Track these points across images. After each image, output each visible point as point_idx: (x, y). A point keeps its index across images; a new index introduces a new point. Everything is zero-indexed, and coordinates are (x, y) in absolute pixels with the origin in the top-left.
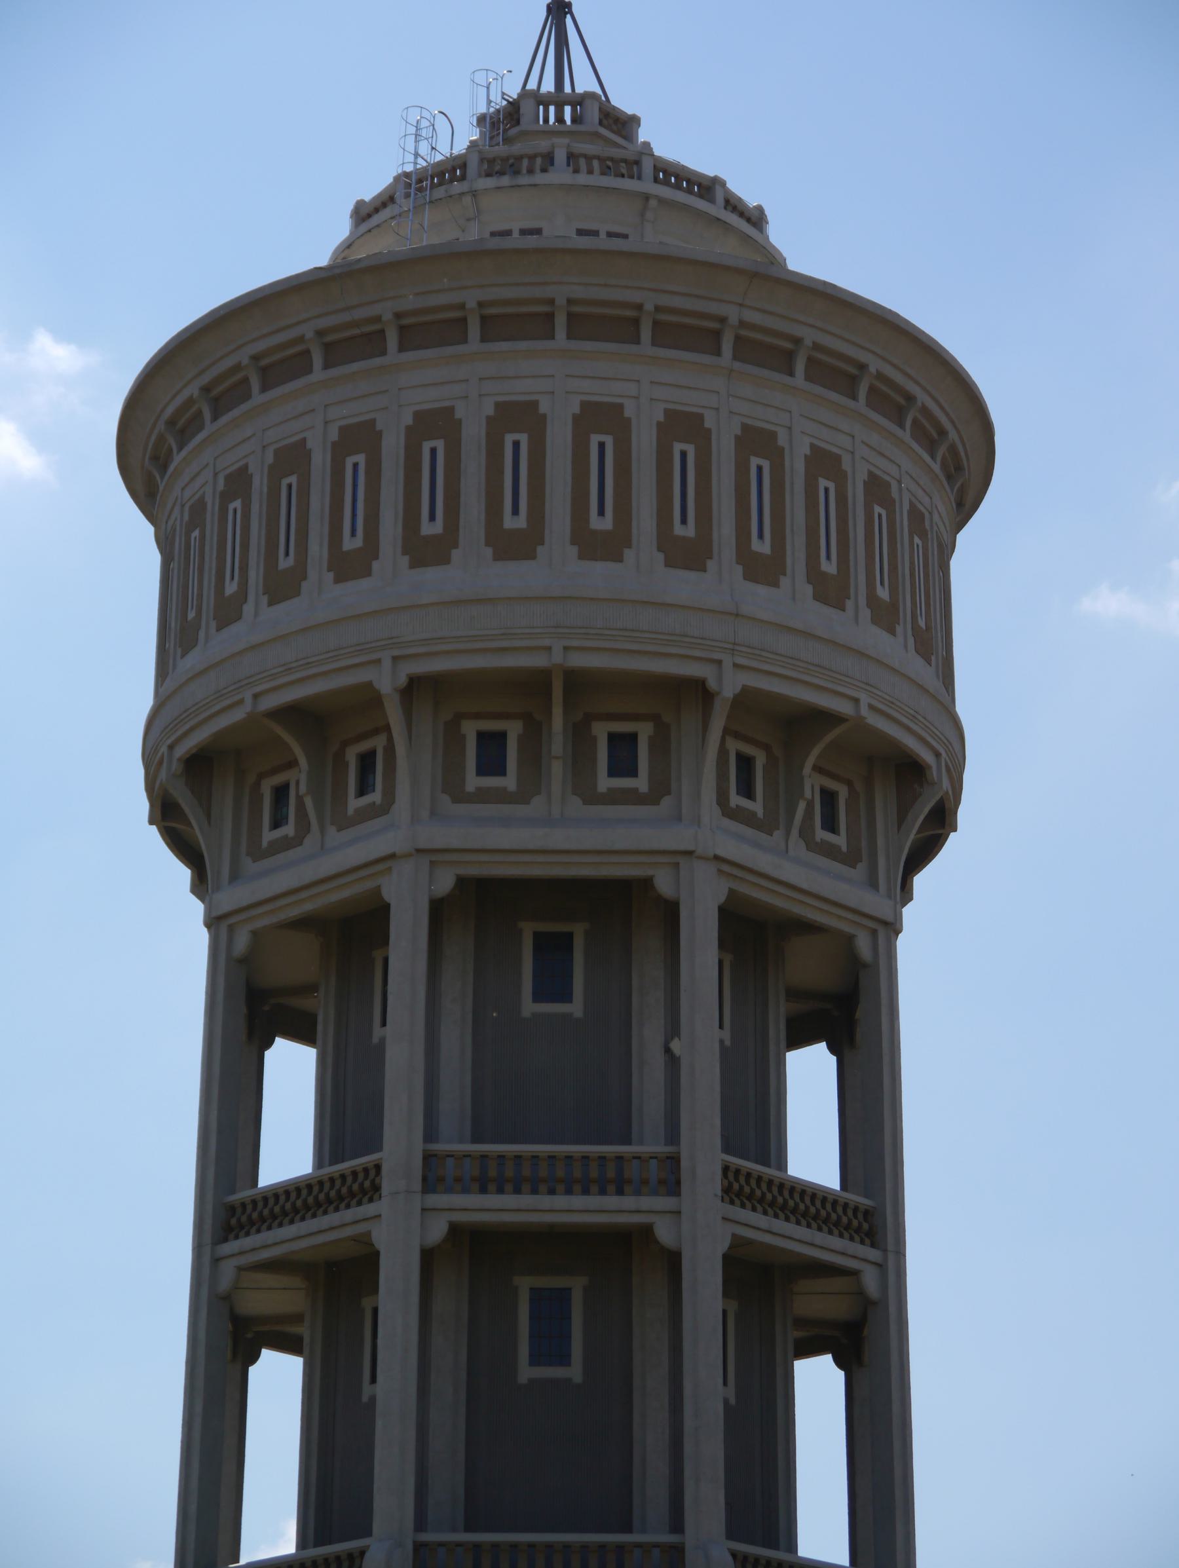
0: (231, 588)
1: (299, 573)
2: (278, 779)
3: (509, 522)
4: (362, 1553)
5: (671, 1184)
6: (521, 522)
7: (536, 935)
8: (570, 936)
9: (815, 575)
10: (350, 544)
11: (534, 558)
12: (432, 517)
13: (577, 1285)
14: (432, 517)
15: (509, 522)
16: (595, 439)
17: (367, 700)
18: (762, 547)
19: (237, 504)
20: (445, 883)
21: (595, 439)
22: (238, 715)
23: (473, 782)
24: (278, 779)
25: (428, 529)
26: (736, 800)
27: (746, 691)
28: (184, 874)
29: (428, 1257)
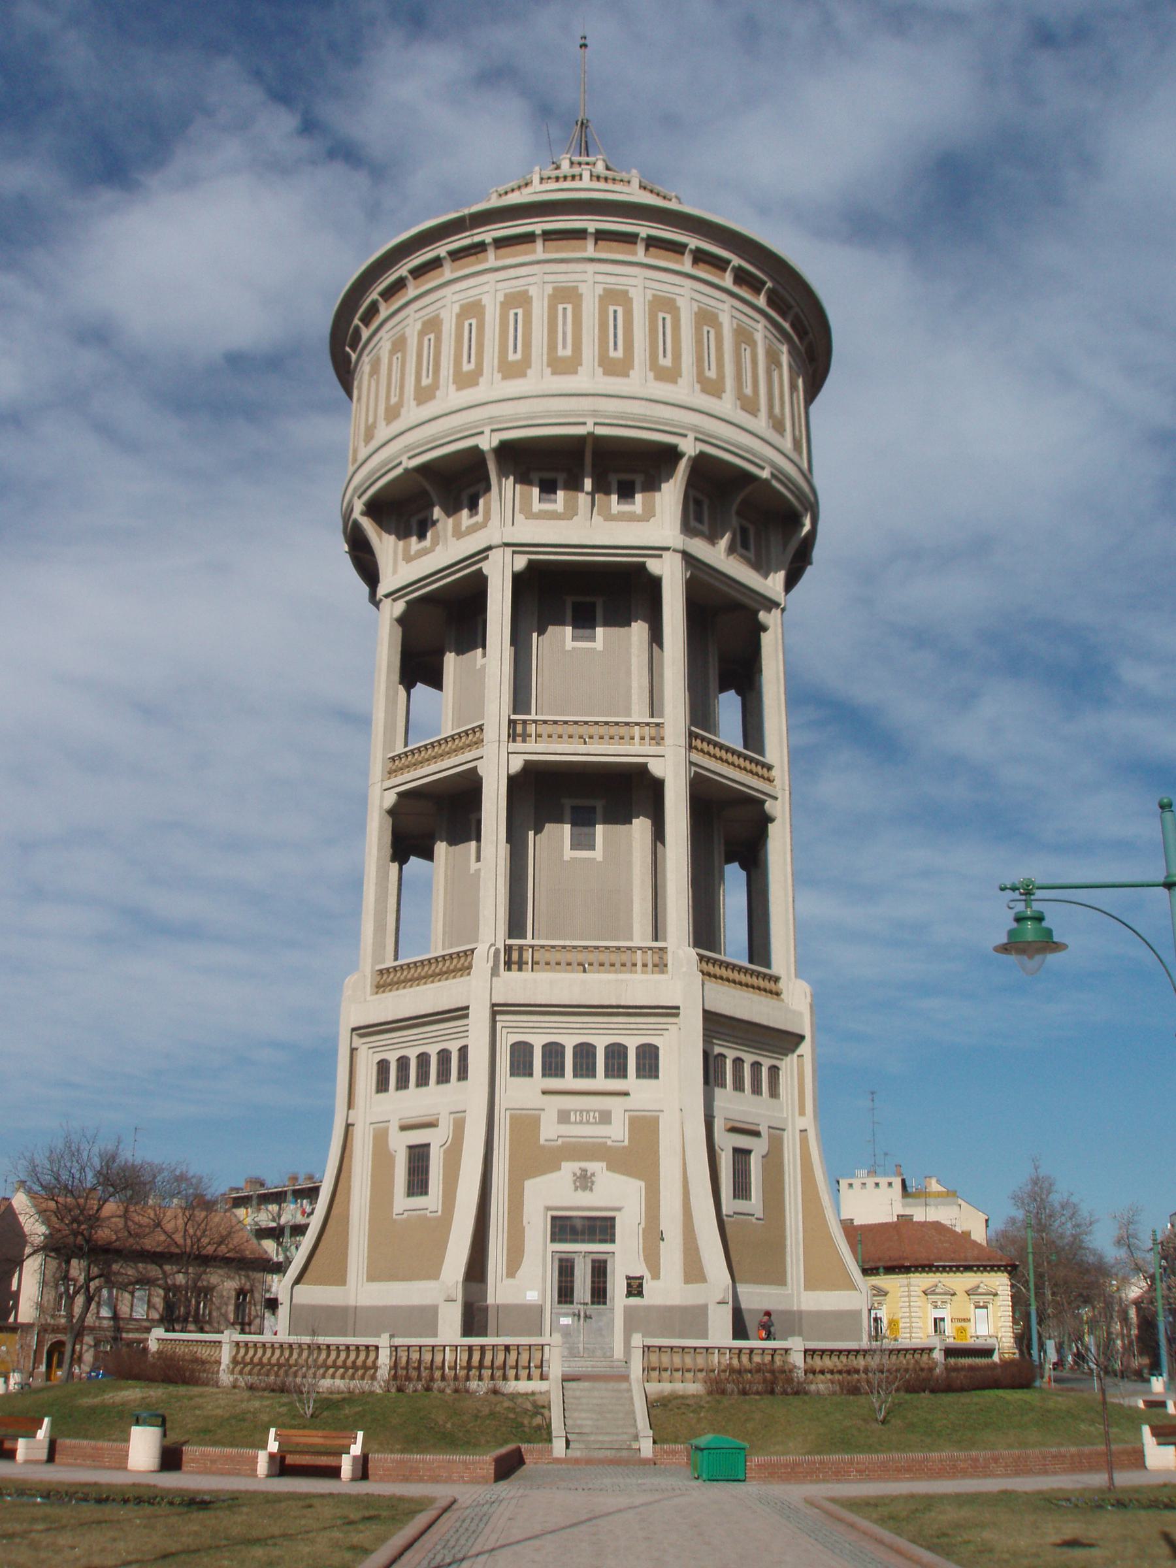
0: (394, 400)
1: (435, 386)
2: (421, 516)
3: (561, 352)
4: (472, 951)
5: (658, 740)
6: (568, 352)
7: (573, 603)
8: (593, 605)
9: (740, 396)
10: (467, 367)
11: (576, 373)
12: (515, 351)
13: (599, 805)
14: (515, 351)
15: (561, 352)
16: (611, 309)
17: (475, 453)
18: (712, 374)
19: (399, 355)
20: (521, 563)
21: (611, 309)
22: (399, 471)
23: (537, 506)
24: (421, 516)
25: (511, 357)
26: (693, 523)
27: (702, 456)
28: (365, 589)
29: (513, 782)
